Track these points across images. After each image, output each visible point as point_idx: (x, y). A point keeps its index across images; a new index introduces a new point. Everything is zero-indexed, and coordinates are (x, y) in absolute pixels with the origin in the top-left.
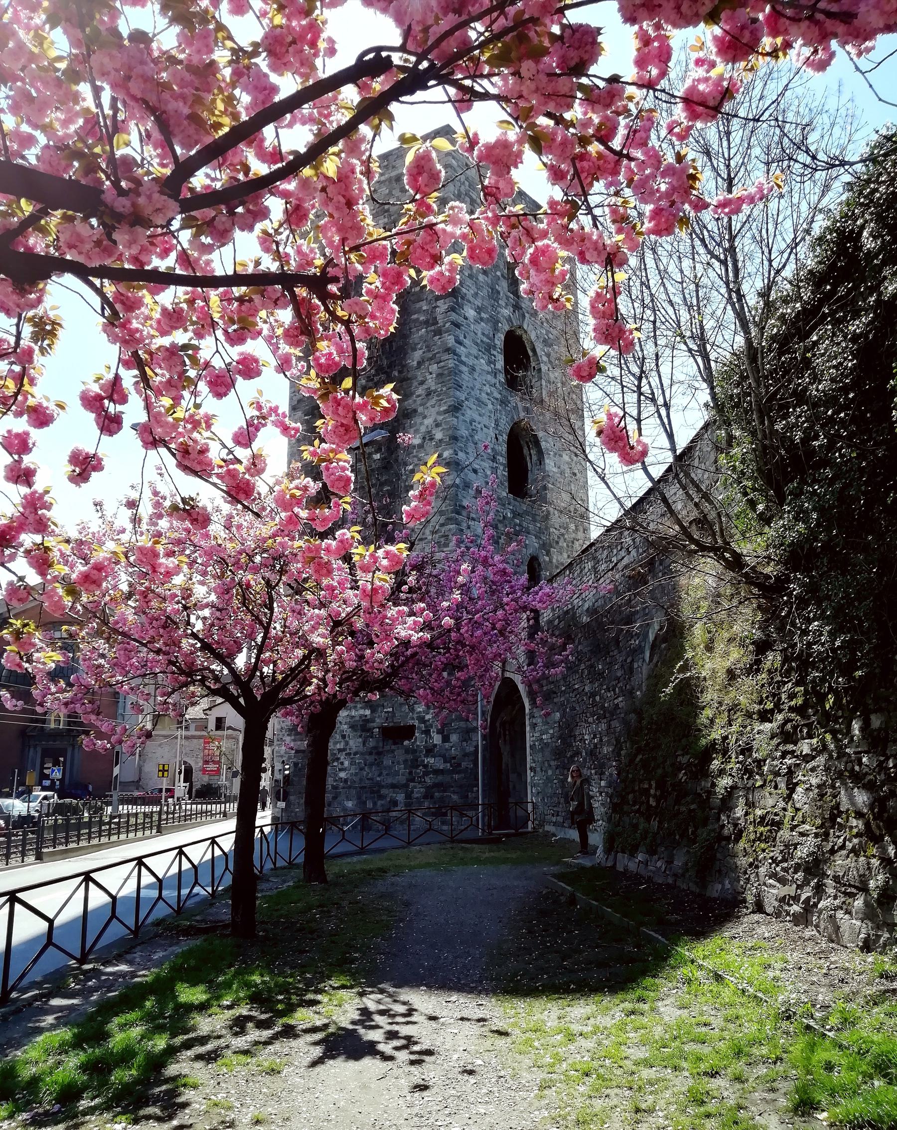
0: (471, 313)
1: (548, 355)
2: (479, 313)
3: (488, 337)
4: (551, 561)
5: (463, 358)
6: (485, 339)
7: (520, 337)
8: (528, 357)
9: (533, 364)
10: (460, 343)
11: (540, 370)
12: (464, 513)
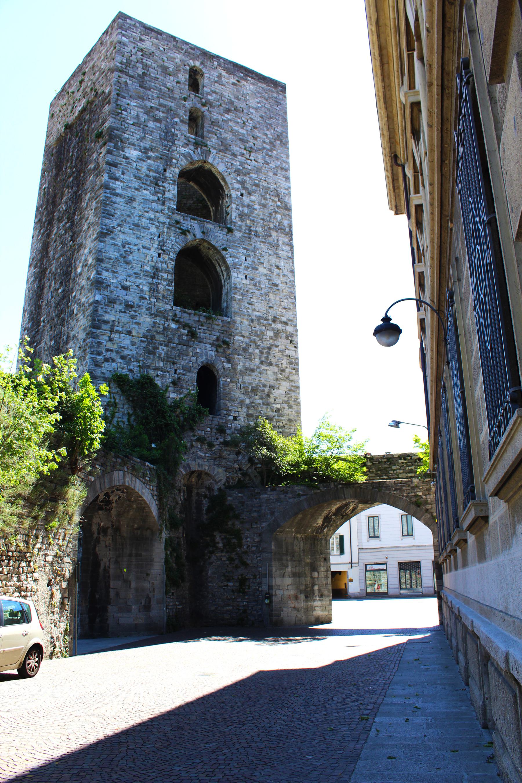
0: (134, 154)
1: (242, 183)
2: (146, 153)
3: (157, 172)
4: (234, 368)
5: (119, 191)
6: (151, 174)
7: (210, 172)
8: (222, 187)
9: (226, 192)
10: (116, 179)
11: (231, 195)
12: (106, 327)
